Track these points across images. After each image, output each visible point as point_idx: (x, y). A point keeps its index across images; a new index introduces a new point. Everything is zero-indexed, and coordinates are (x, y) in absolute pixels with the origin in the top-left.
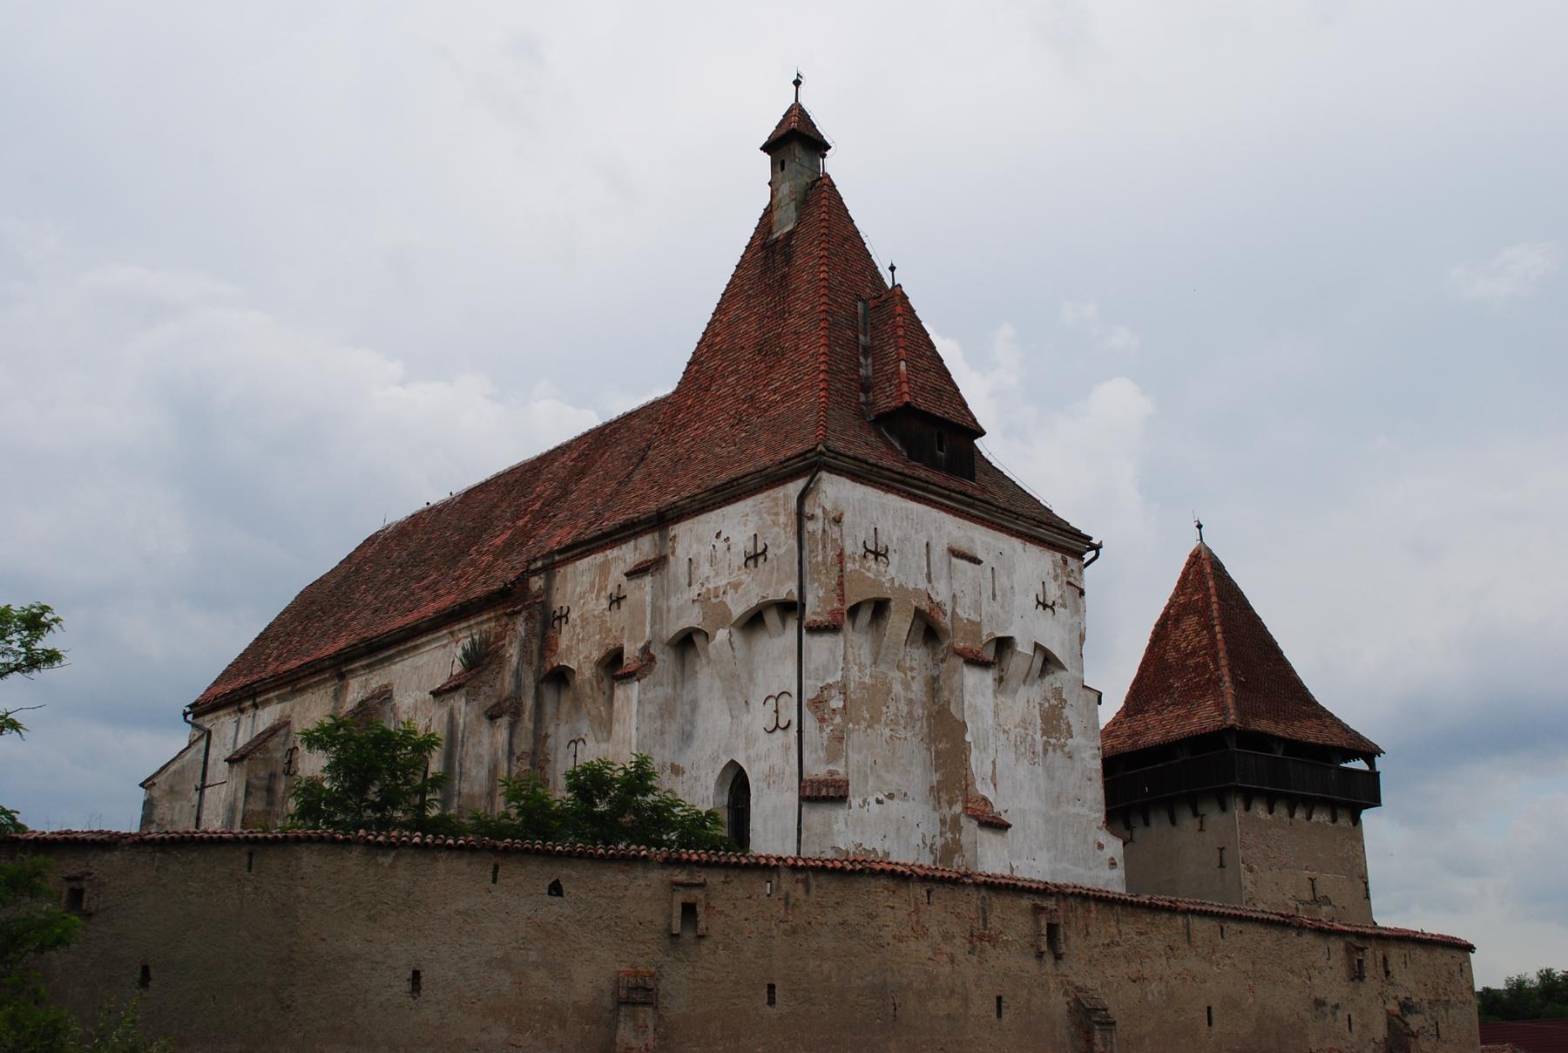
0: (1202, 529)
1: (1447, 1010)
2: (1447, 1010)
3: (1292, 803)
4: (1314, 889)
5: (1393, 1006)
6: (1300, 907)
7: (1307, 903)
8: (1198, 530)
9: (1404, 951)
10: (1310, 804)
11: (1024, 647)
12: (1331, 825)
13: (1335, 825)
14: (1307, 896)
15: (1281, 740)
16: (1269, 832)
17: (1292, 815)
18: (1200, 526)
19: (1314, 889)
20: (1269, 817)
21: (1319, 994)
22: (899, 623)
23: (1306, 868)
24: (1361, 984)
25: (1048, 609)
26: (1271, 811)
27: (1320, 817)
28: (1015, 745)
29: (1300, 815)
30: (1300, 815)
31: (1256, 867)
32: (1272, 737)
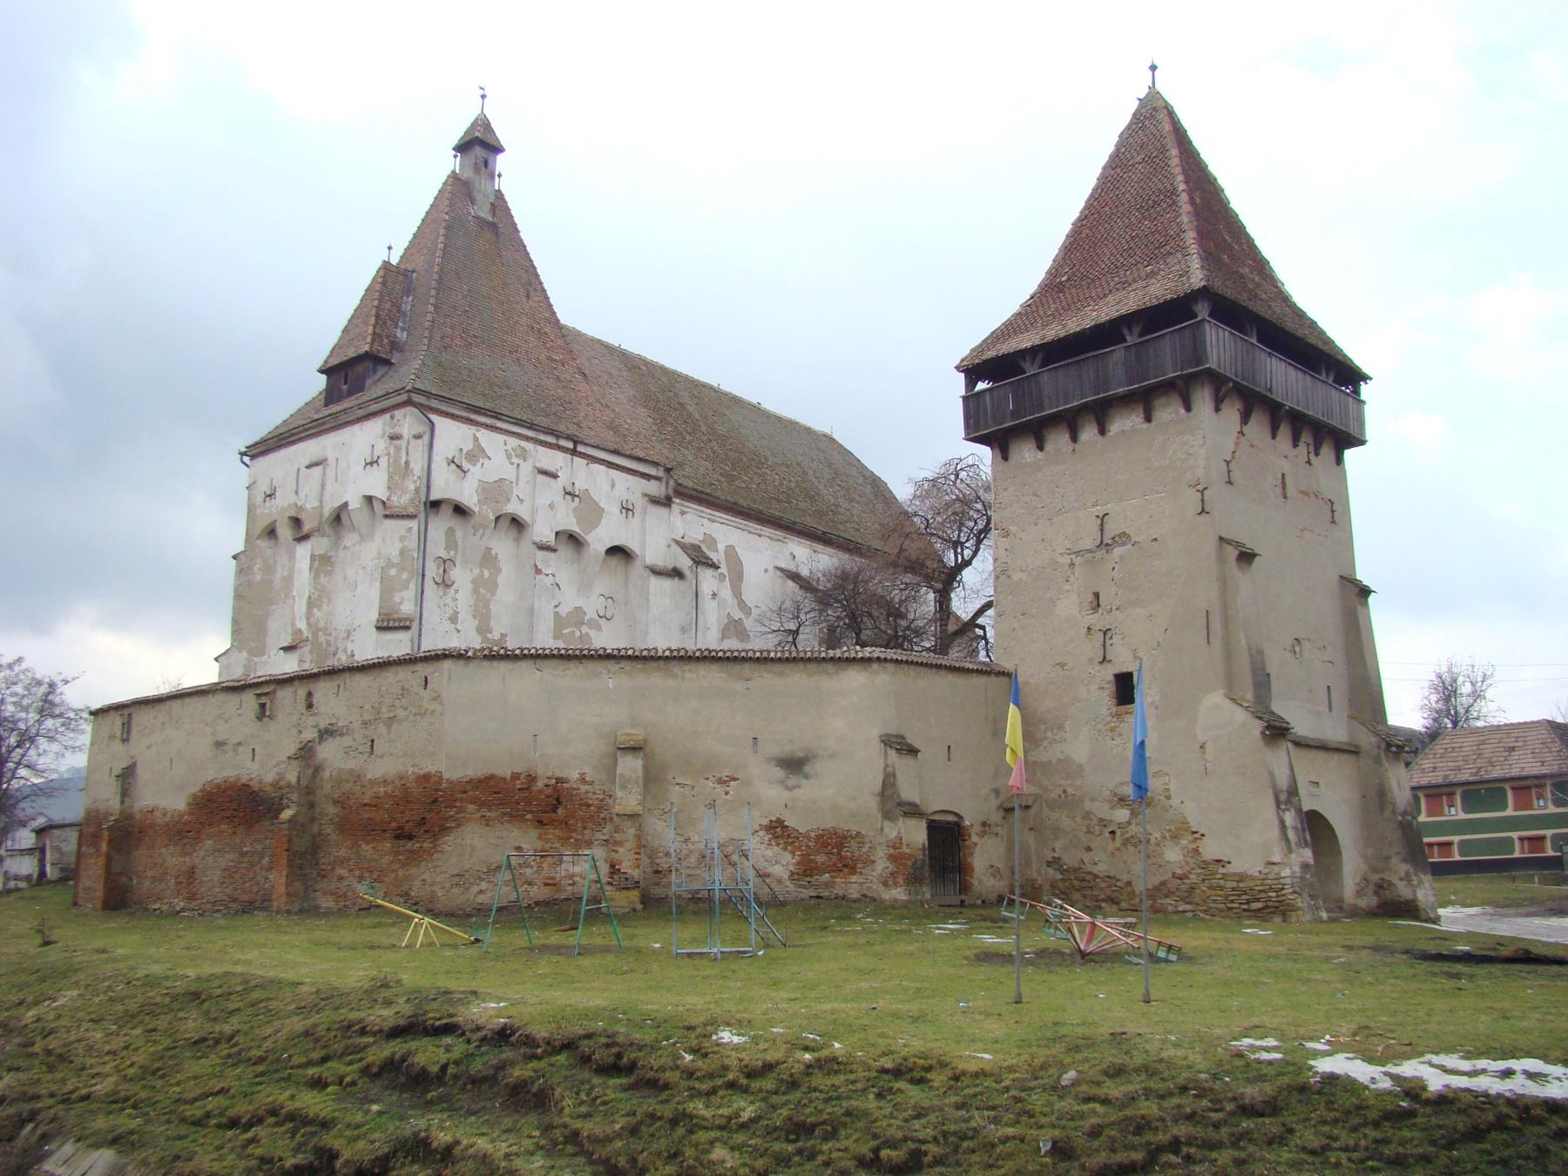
0: (1156, 72)
1: (389, 727)
2: (389, 727)
3: (1071, 422)
4: (1102, 530)
5: (310, 734)
6: (1078, 560)
7: (1090, 551)
8: (1150, 73)
9: (336, 683)
10: (1101, 412)
11: (355, 503)
12: (1145, 426)
13: (1154, 423)
14: (1089, 542)
15: (1033, 351)
16: (1040, 475)
17: (1074, 439)
18: (1153, 68)
19: (1102, 530)
20: (1040, 455)
21: (221, 737)
22: (285, 532)
23: (1095, 505)
24: (272, 723)
25: (375, 465)
26: (1041, 448)
27: (1126, 423)
28: (372, 575)
29: (1089, 433)
30: (1089, 433)
31: (1013, 528)
32: (1022, 353)
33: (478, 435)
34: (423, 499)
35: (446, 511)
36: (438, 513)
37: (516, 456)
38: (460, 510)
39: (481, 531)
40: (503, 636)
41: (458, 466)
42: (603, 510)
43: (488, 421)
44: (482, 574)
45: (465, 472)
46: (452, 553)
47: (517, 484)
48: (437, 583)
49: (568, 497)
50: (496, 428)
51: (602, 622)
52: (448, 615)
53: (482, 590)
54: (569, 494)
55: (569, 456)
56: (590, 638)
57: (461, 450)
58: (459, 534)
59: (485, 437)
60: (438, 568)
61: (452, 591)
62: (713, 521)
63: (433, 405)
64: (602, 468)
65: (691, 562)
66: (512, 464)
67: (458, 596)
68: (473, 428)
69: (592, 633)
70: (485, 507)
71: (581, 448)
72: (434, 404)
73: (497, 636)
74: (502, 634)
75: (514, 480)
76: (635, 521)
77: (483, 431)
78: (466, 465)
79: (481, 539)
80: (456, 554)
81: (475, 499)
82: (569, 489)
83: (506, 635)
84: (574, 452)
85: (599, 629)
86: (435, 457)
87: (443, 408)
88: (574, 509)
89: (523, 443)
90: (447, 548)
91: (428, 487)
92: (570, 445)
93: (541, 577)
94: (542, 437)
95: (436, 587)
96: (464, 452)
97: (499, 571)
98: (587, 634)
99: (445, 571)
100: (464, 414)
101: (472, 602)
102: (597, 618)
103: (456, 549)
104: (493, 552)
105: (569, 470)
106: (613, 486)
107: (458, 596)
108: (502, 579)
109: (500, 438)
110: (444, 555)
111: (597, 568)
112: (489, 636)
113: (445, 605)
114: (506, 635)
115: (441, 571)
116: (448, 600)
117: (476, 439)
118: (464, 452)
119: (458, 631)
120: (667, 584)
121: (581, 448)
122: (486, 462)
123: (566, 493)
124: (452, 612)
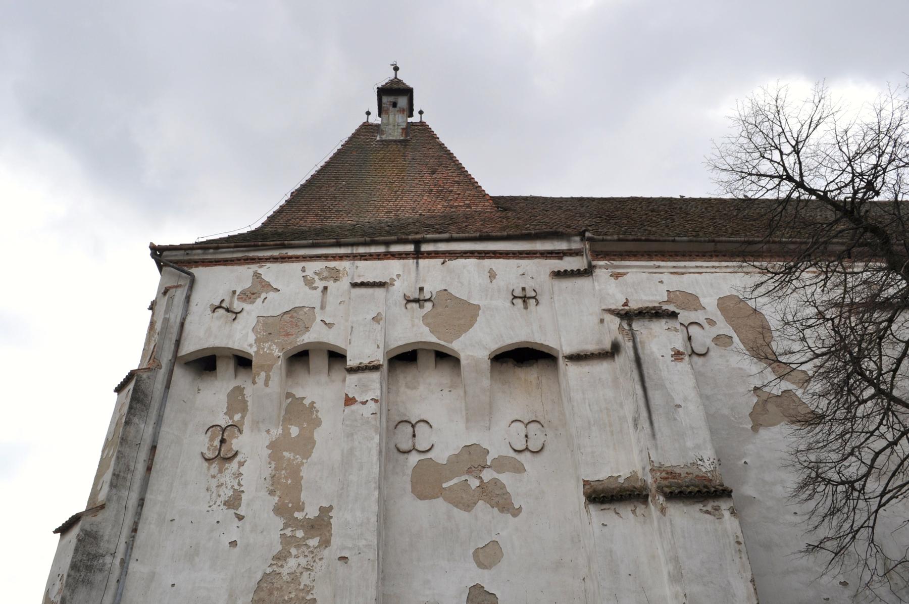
33: (260, 271)
34: (166, 357)
35: (225, 369)
36: (216, 376)
37: (321, 279)
38: (243, 362)
39: (263, 374)
40: (325, 511)
41: (228, 310)
42: (478, 307)
43: (276, 253)
44: (286, 433)
45: (237, 313)
46: (237, 417)
47: (323, 307)
48: (206, 460)
49: (410, 305)
50: (290, 257)
51: (524, 458)
52: (224, 498)
53: (286, 454)
54: (417, 301)
55: (411, 262)
56: (503, 487)
57: (234, 292)
58: (249, 391)
59: (270, 272)
60: (212, 439)
61: (234, 464)
62: (683, 274)
63: (196, 257)
64: (472, 262)
65: (617, 320)
66: (315, 288)
67: (242, 470)
68: (254, 267)
69: (505, 478)
70: (267, 345)
71: (425, 248)
72: (198, 255)
73: (312, 512)
74: (322, 509)
75: (318, 305)
76: (536, 311)
77: (268, 265)
78: (237, 306)
79: (266, 384)
80: (243, 417)
81: (252, 338)
82: (416, 295)
83: (331, 508)
84: (418, 255)
85: (519, 469)
86: (193, 307)
87: (209, 257)
88: (425, 317)
89: (333, 264)
90: (230, 412)
91: (178, 343)
92: (410, 248)
93: (354, 407)
94: (362, 250)
95: (206, 464)
96: (238, 293)
97: (318, 423)
98: (496, 482)
99: (223, 441)
100: (239, 255)
101: (267, 472)
102: (512, 454)
103: (244, 410)
104: (307, 402)
105: (413, 274)
106: (492, 275)
107: (242, 470)
108: (318, 435)
109: (298, 266)
110: (223, 421)
111: (486, 382)
112: (299, 515)
113: (219, 486)
114: (331, 508)
115: (217, 443)
116: (227, 478)
117: (257, 275)
118: (238, 293)
119: (240, 518)
120: (602, 368)
121: (425, 248)
122: (271, 295)
123: (409, 301)
124: (231, 493)
